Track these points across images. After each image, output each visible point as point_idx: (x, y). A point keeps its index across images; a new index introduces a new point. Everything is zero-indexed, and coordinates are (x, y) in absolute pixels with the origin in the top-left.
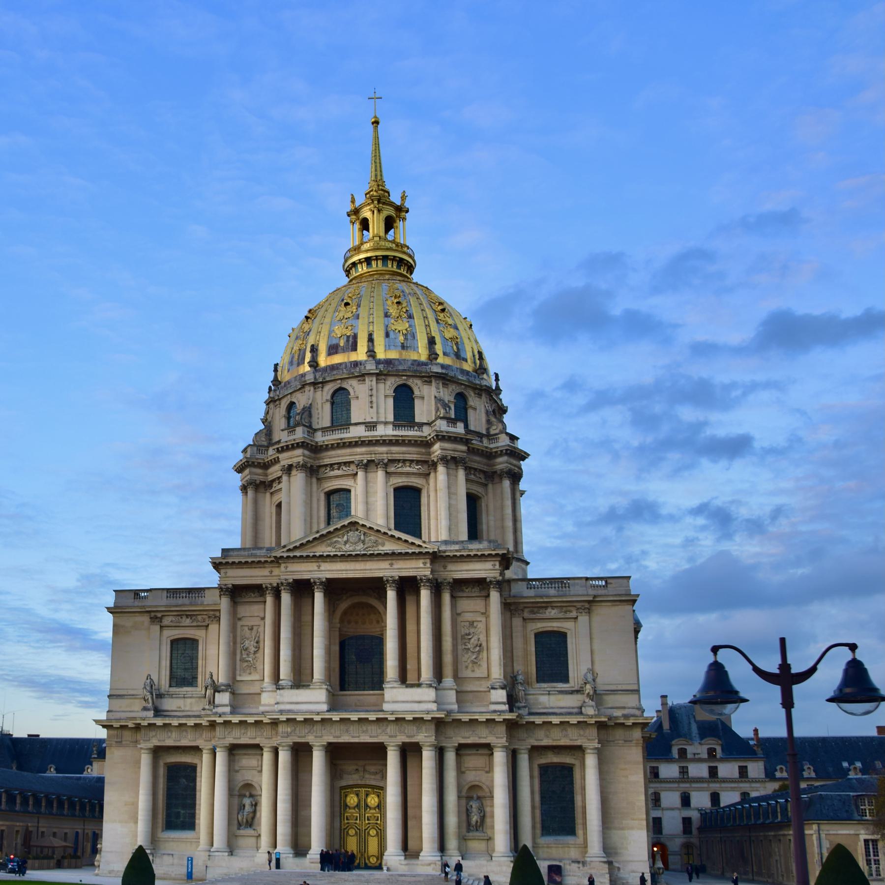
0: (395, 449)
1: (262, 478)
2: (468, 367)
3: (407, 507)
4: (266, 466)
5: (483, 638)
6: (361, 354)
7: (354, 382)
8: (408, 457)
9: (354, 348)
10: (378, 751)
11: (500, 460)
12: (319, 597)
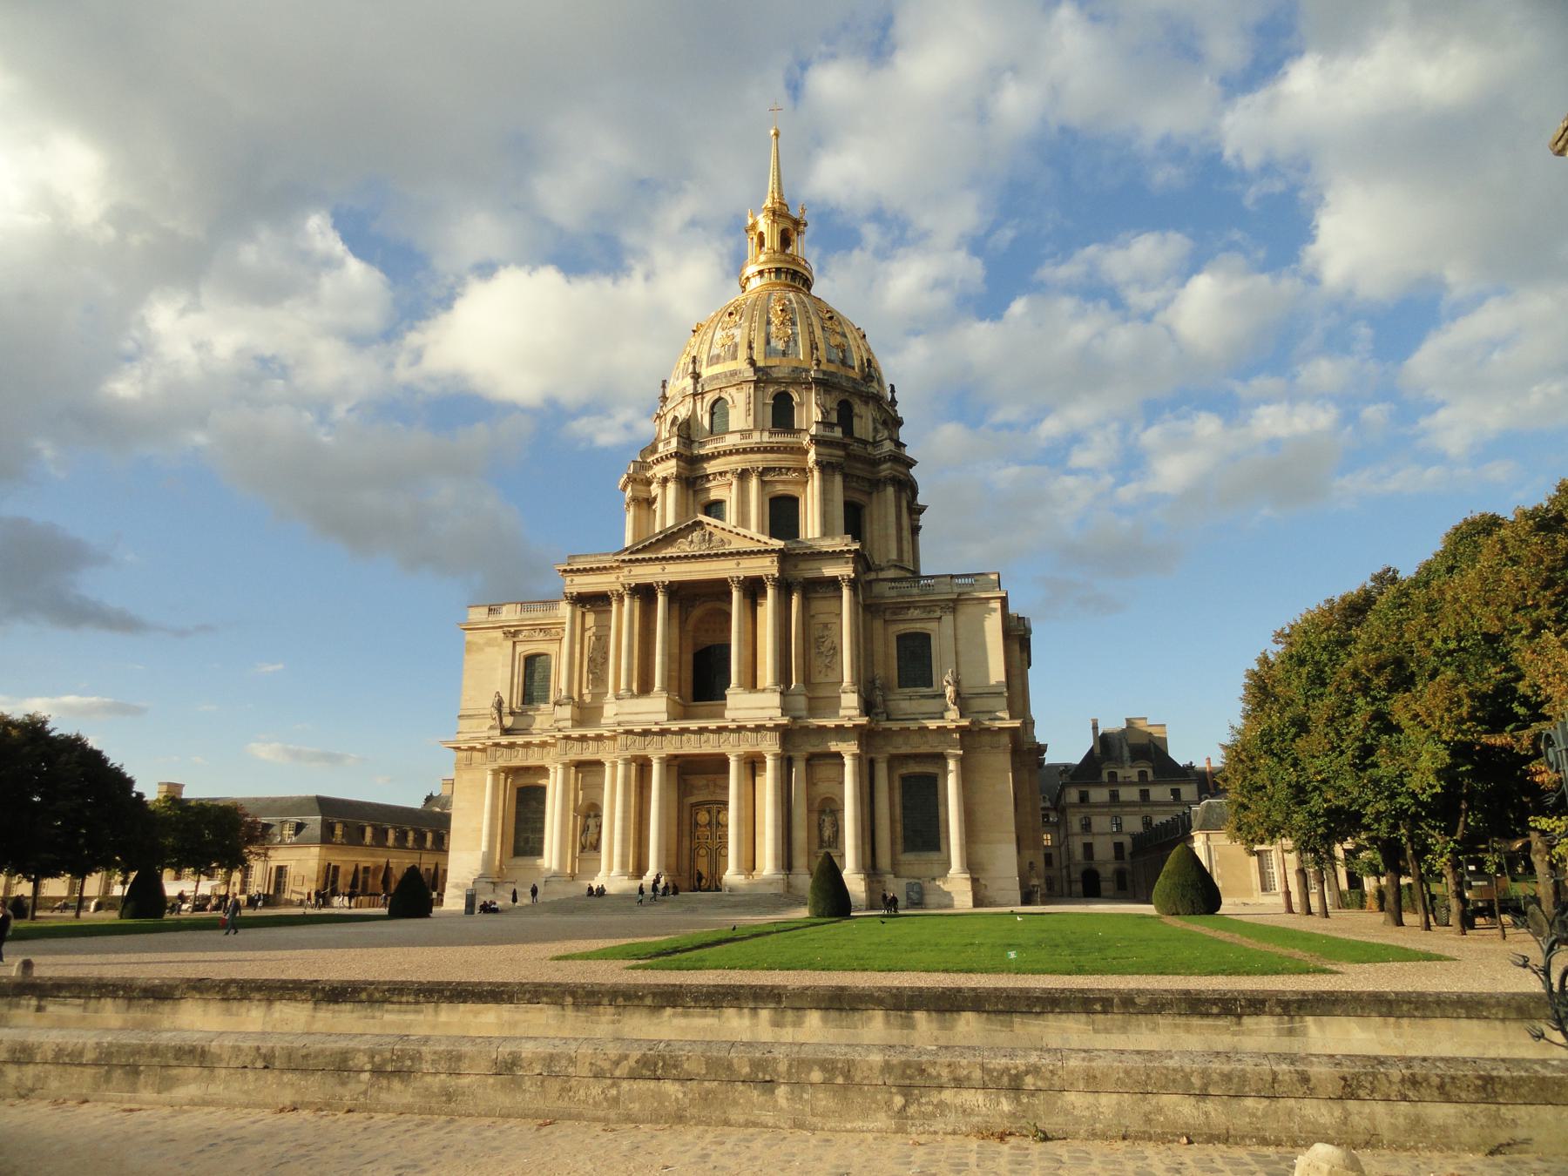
0: (770, 456)
1: (645, 495)
2: (856, 373)
3: (782, 515)
4: (649, 483)
5: (836, 640)
6: (741, 364)
7: (733, 391)
8: (783, 464)
9: (735, 358)
10: (721, 763)
11: (884, 466)
12: (661, 599)
